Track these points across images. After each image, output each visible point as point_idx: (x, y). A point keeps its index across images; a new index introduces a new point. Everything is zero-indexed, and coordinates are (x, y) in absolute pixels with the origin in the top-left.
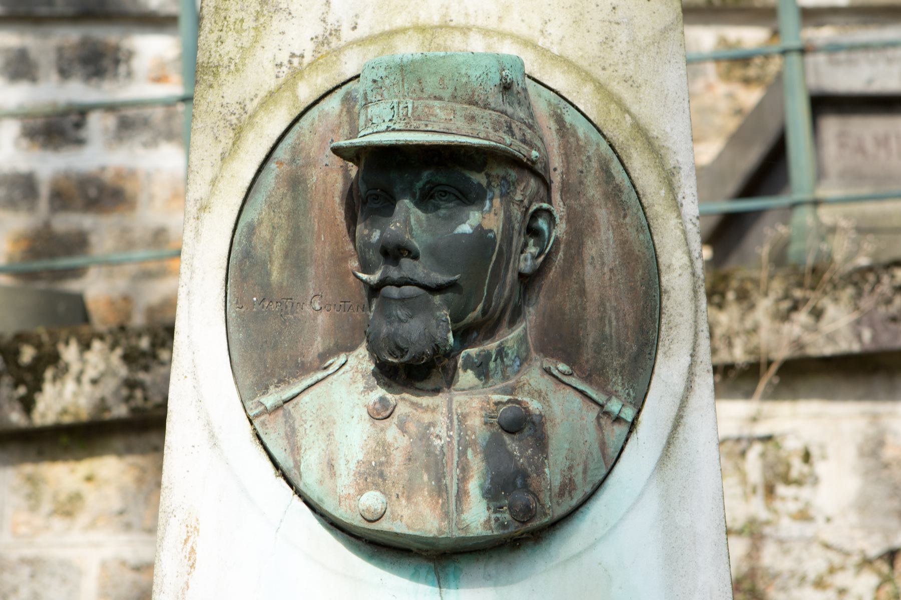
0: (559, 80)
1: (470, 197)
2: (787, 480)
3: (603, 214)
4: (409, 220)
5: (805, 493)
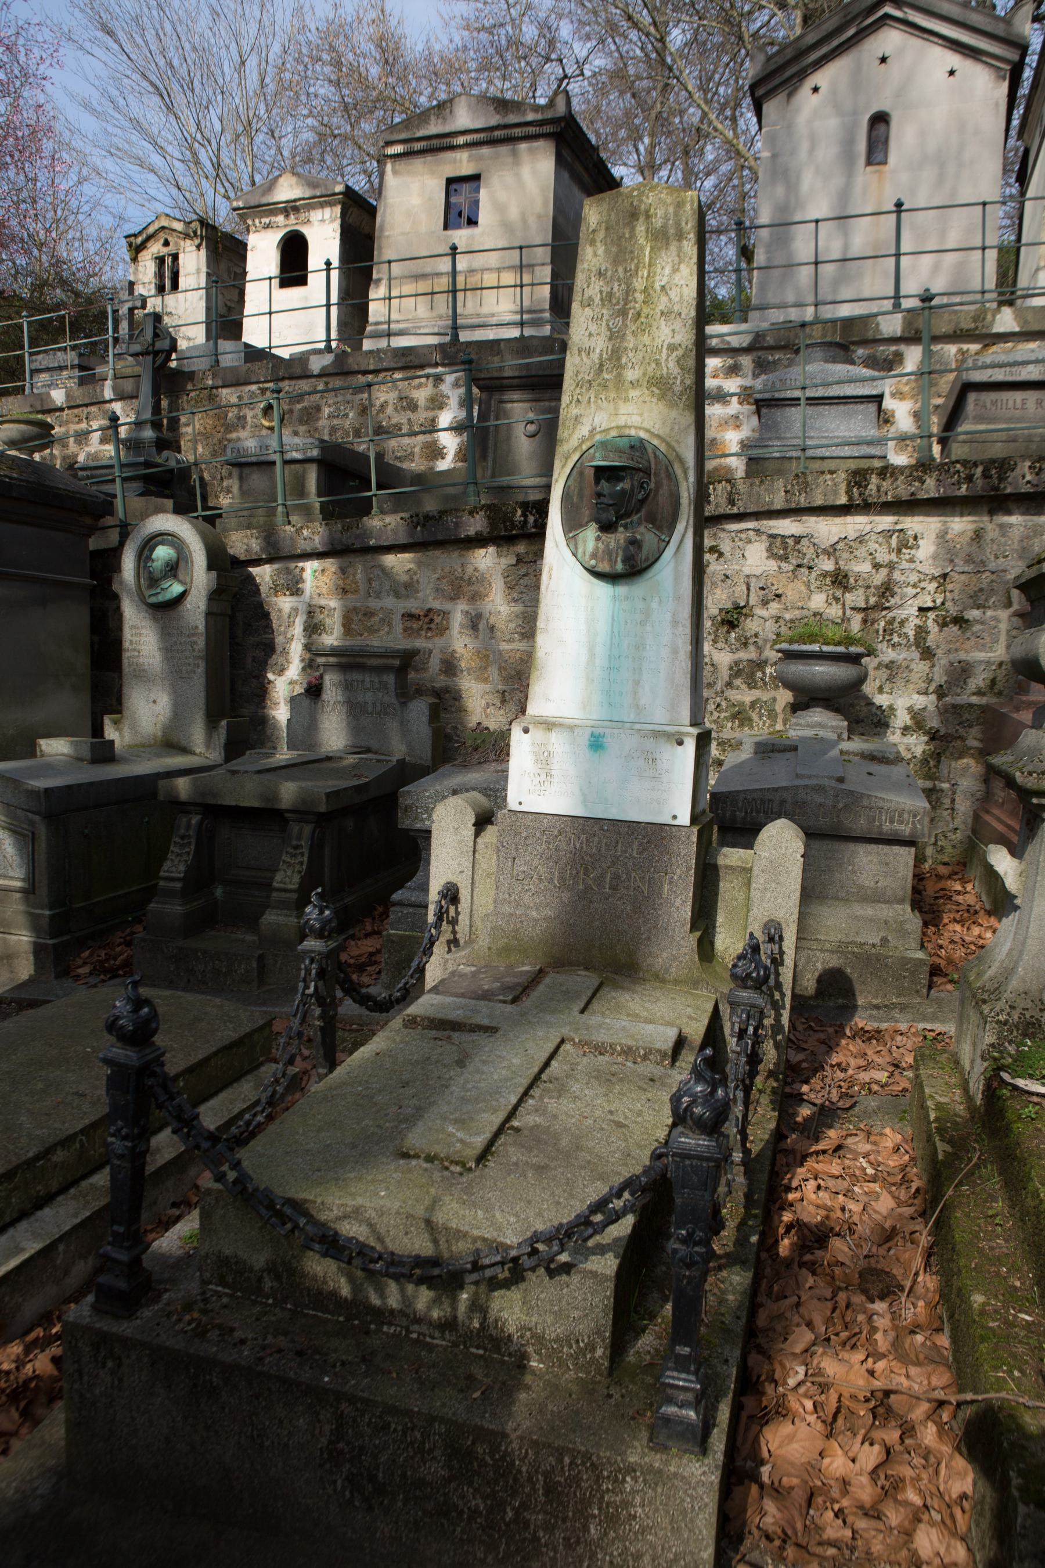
0: (656, 442)
1: (621, 479)
2: (907, 548)
3: (665, 482)
4: (604, 485)
5: (913, 552)
